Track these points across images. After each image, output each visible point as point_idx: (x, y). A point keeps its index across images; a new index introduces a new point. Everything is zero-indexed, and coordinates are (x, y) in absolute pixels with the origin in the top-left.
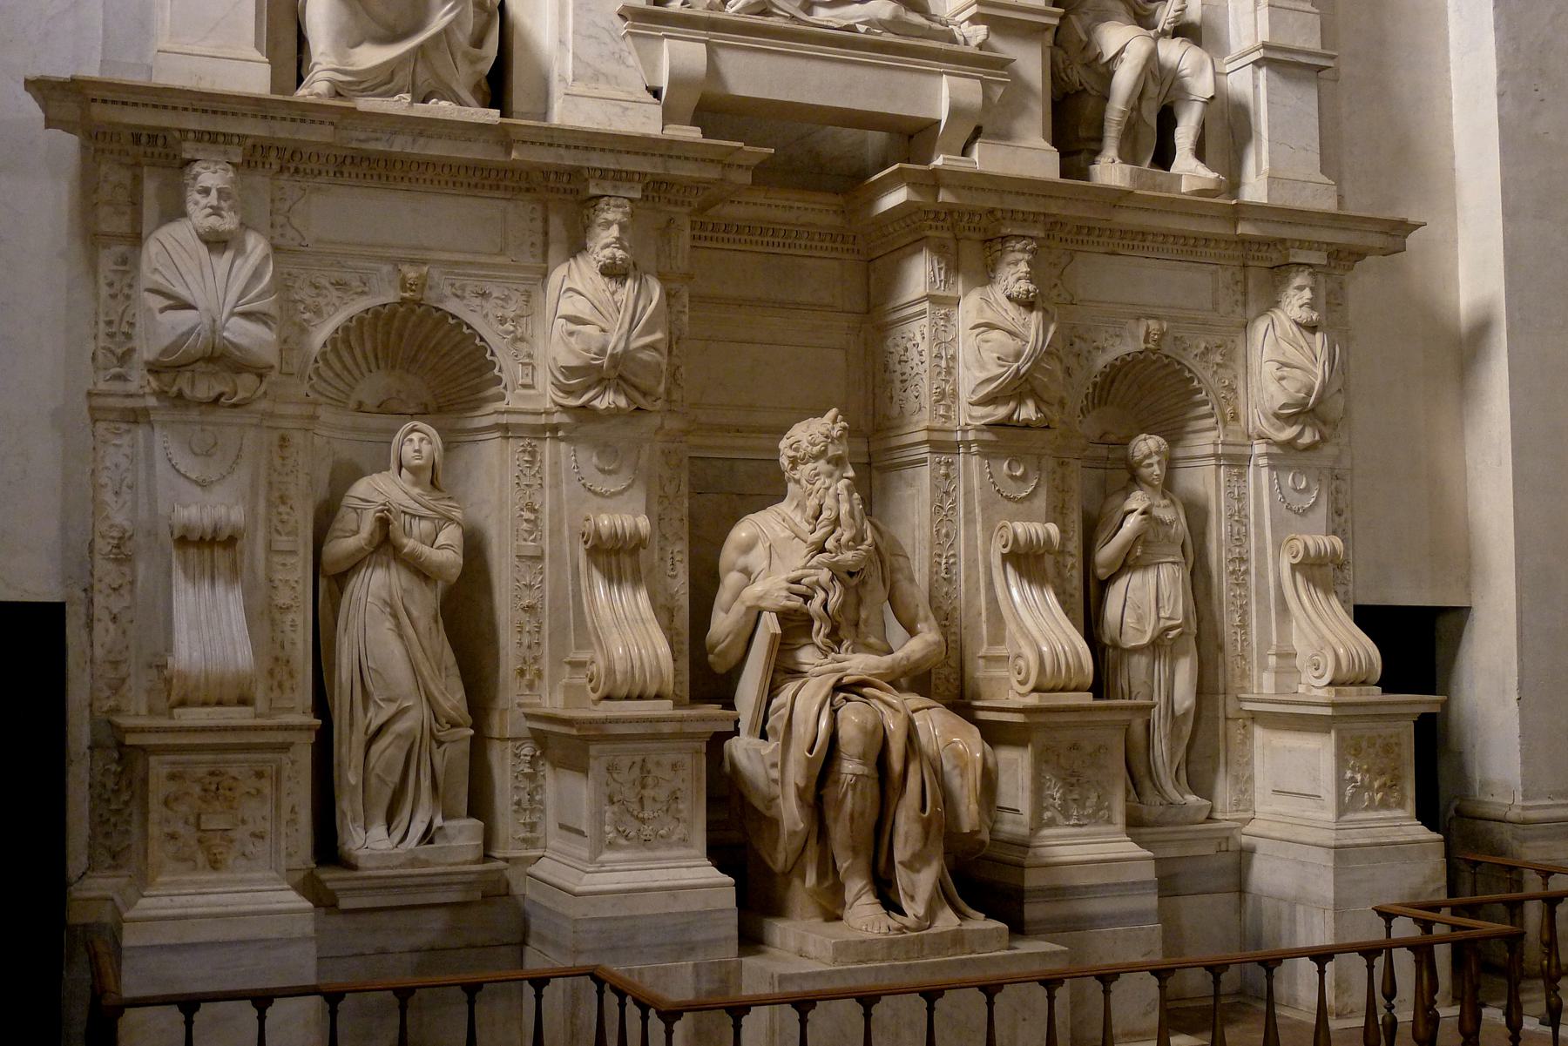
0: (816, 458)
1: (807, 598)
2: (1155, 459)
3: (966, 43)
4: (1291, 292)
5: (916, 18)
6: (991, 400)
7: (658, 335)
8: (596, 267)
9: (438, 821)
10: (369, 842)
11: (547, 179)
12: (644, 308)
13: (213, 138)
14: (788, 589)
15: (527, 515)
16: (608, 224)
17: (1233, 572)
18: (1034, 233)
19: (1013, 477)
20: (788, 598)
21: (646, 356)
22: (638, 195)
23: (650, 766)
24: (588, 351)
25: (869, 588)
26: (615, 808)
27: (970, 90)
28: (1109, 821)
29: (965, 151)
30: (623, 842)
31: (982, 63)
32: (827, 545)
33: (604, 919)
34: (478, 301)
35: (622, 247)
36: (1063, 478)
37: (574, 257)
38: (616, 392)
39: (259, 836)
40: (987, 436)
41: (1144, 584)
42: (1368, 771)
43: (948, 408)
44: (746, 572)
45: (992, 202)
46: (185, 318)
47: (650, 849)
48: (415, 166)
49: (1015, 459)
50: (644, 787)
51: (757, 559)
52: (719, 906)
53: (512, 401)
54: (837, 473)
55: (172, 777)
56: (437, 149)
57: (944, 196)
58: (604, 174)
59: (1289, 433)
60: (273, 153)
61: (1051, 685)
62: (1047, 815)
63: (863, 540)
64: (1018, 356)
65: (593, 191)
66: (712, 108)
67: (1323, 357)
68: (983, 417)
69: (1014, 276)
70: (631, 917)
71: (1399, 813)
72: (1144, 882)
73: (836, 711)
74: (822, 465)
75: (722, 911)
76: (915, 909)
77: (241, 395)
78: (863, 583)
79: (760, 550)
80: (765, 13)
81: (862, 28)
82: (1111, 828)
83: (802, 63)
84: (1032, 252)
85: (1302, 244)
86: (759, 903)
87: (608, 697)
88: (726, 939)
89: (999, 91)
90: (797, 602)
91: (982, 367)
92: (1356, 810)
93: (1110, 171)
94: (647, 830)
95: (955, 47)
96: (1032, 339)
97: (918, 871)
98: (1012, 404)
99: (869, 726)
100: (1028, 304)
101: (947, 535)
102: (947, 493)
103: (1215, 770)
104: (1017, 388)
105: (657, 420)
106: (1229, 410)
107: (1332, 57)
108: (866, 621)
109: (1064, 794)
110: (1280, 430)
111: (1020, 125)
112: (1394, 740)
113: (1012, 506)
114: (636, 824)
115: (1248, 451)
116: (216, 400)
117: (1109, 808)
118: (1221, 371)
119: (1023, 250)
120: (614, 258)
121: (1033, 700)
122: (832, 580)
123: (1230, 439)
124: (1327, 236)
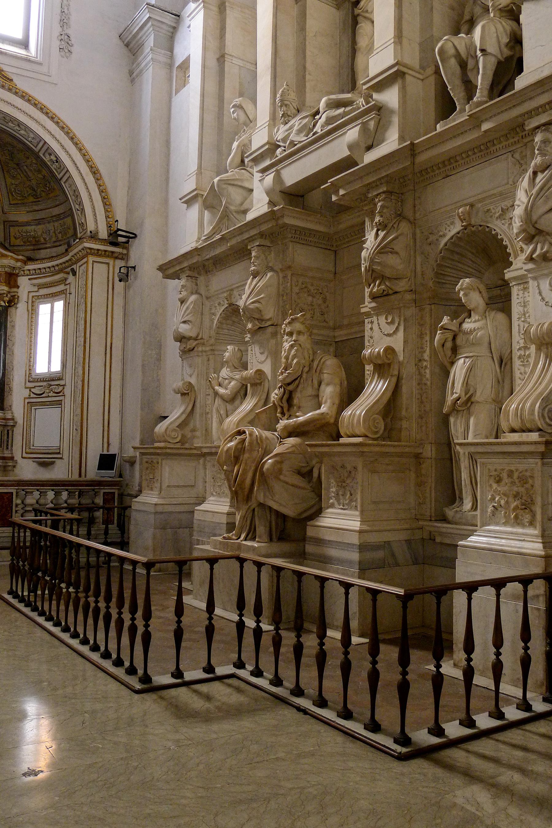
2: (462, 293)
17: (520, 357)
18: (381, 190)
19: (387, 323)
21: (252, 306)
22: (258, 244)
27: (352, 134)
36: (422, 318)
42: (505, 495)
47: (220, 497)
49: (388, 312)
65: (249, 248)
72: (354, 545)
78: (298, 386)
83: (304, 160)
85: (530, 114)
89: (372, 124)
92: (497, 524)
102: (371, 337)
112: (528, 474)
117: (356, 501)
119: (379, 201)
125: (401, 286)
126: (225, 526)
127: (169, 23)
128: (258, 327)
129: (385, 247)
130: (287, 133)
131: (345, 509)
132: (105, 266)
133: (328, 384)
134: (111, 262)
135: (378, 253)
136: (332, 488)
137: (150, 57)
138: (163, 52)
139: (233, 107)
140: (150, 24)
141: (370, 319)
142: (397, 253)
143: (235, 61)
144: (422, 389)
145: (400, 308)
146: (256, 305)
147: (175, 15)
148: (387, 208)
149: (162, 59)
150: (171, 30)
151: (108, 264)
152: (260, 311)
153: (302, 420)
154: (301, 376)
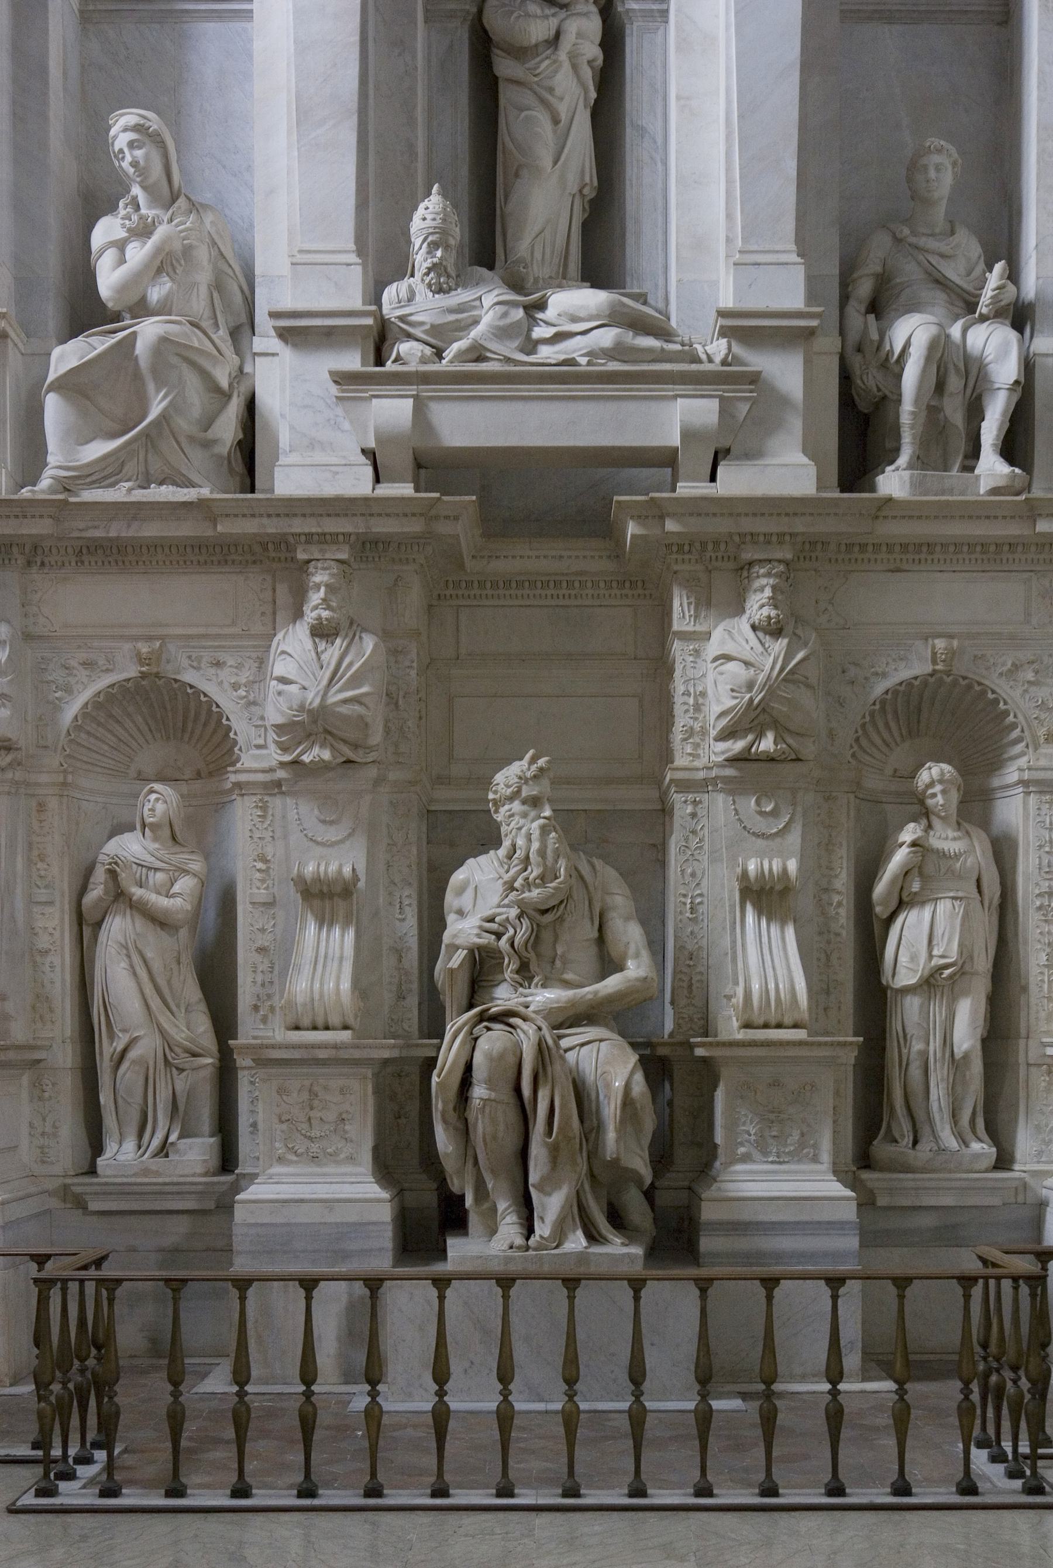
0: (511, 799)
1: (499, 936)
6: (728, 734)
7: (364, 689)
8: (308, 632)
11: (266, 549)
12: (351, 664)
14: (480, 927)
16: (318, 587)
20: (478, 936)
21: (344, 709)
23: (315, 1088)
24: (291, 709)
25: (566, 924)
26: (284, 1126)
28: (815, 1159)
29: (713, 478)
30: (295, 1158)
32: (517, 885)
33: (262, 1225)
35: (329, 608)
37: (294, 622)
38: (322, 746)
44: (461, 913)
47: (319, 1165)
48: (144, 550)
50: (312, 1109)
51: (466, 901)
52: (374, 1219)
54: (533, 814)
60: (15, 550)
61: (761, 1022)
62: (742, 1150)
63: (556, 878)
64: (750, 685)
66: (433, 466)
68: (723, 753)
69: (759, 604)
70: (288, 1224)
73: (476, 1039)
74: (516, 806)
75: (374, 1223)
76: (543, 1229)
78: (561, 919)
79: (469, 893)
84: (776, 575)
86: (429, 1223)
87: (297, 1028)
88: (380, 1250)
90: (488, 939)
91: (718, 701)
93: (894, 482)
94: (314, 1148)
96: (768, 668)
97: (550, 1194)
98: (750, 737)
99: (502, 1056)
100: (772, 630)
103: (1016, 1120)
104: (751, 719)
108: (563, 956)
109: (761, 1130)
111: (774, 443)
114: (307, 1142)
117: (815, 1146)
119: (768, 575)
120: (319, 618)
121: (741, 1035)
122: (519, 917)
125: (809, 749)
126: (390, 1228)
128: (344, 759)
129: (792, 672)
131: (784, 1162)
133: (627, 919)
135: (784, 680)
136: (744, 1124)
142: (808, 686)
146: (357, 708)
148: (782, 593)
152: (367, 724)
153: (610, 990)
154: (569, 897)
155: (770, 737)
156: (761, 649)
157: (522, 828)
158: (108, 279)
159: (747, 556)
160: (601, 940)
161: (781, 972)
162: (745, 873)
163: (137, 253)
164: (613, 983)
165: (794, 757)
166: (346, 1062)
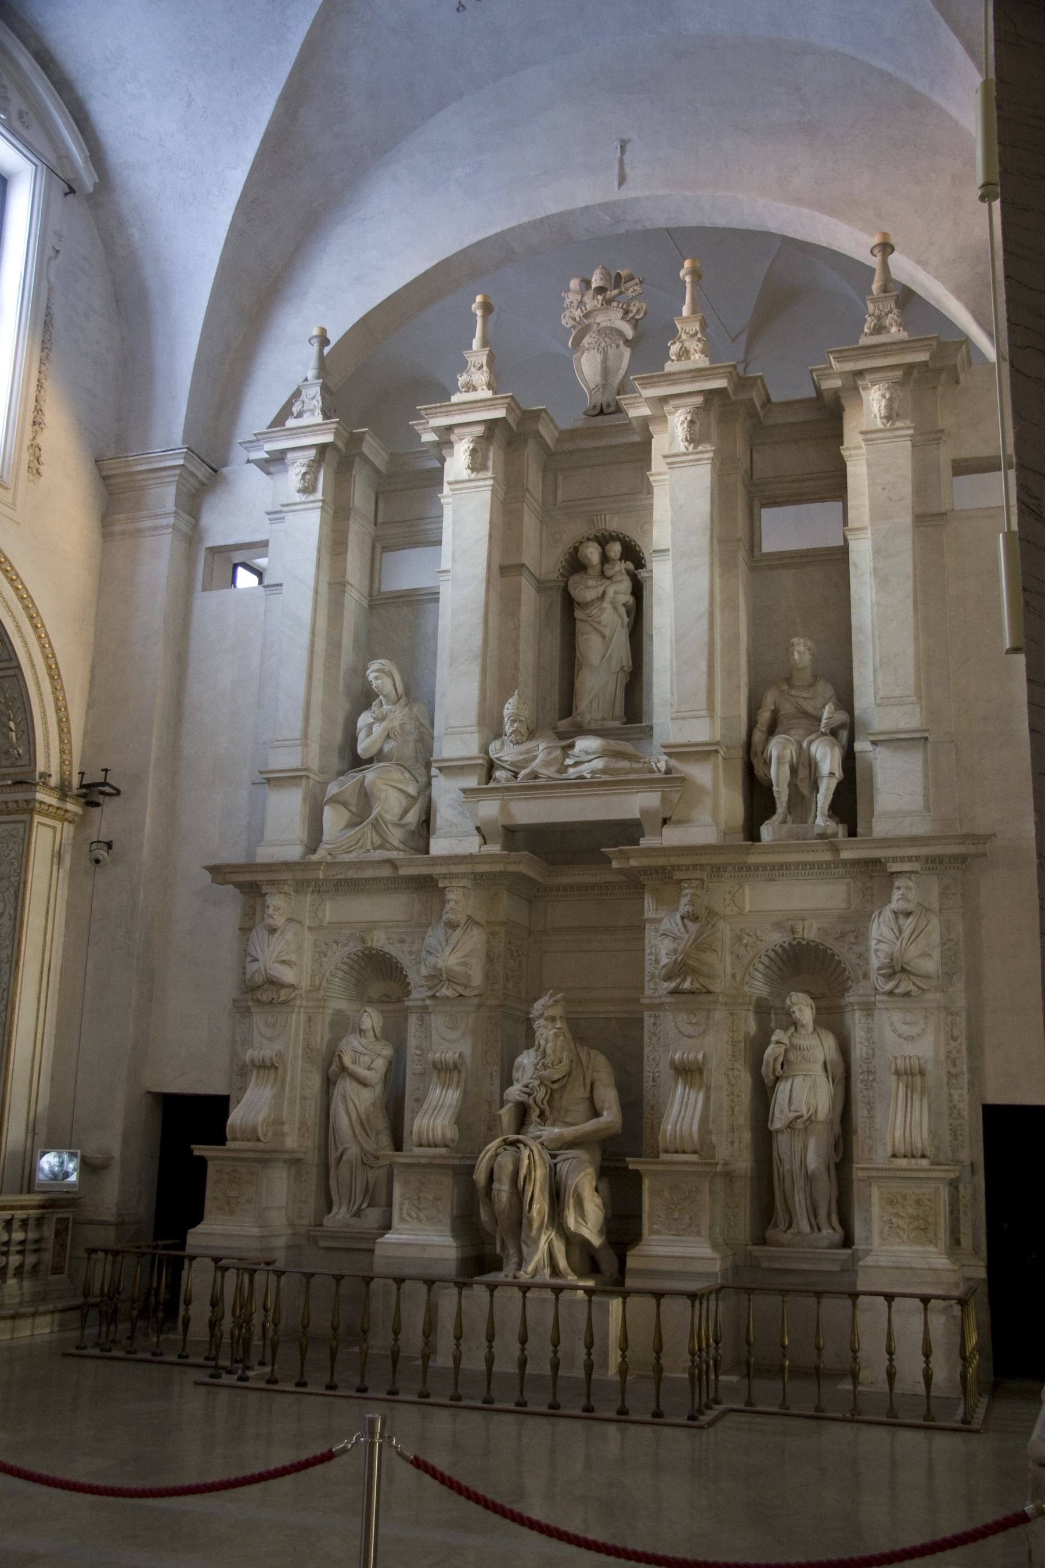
3: (659, 771)
4: (895, 891)
5: (624, 764)
6: (668, 978)
9: (364, 1206)
10: (340, 1214)
13: (271, 882)
15: (418, 1052)
17: (862, 1081)
21: (457, 968)
28: (698, 1234)
31: (670, 779)
33: (387, 1257)
34: (399, 945)
39: (249, 1201)
40: (669, 1000)
41: (785, 1089)
43: (656, 984)
45: (661, 862)
46: (255, 965)
53: (415, 995)
55: (218, 1171)
56: (367, 874)
57: (633, 863)
58: (445, 876)
59: (890, 985)
64: (675, 951)
65: (441, 885)
67: (906, 934)
71: (931, 1248)
77: (282, 999)
78: (564, 1086)
79: (521, 1071)
80: (536, 777)
81: (589, 776)
82: (698, 1239)
85: (895, 860)
89: (676, 797)
90: (524, 1098)
93: (767, 831)
95: (649, 776)
98: (678, 981)
101: (654, 1059)
102: (654, 1034)
105: (476, 1001)
106: (860, 973)
107: (928, 731)
110: (885, 984)
113: (689, 1040)
115: (873, 999)
116: (271, 1002)
118: (855, 947)
123: (861, 992)
124: (912, 852)
127: (201, 477)
130: (521, 757)
132: (50, 831)
134: (58, 825)
137: (171, 520)
138: (187, 517)
139: (377, 671)
140: (178, 472)
141: (652, 1013)
143: (355, 594)
144: (733, 1101)
145: (708, 1010)
147: (213, 469)
149: (183, 527)
150: (197, 485)
151: (54, 828)
155: (689, 980)
156: (683, 930)
157: (546, 1033)
158: (363, 746)
159: (678, 875)
160: (591, 1099)
161: (687, 1119)
162: (672, 1063)
163: (378, 729)
164: (591, 1125)
165: (704, 990)
166: (439, 1166)
